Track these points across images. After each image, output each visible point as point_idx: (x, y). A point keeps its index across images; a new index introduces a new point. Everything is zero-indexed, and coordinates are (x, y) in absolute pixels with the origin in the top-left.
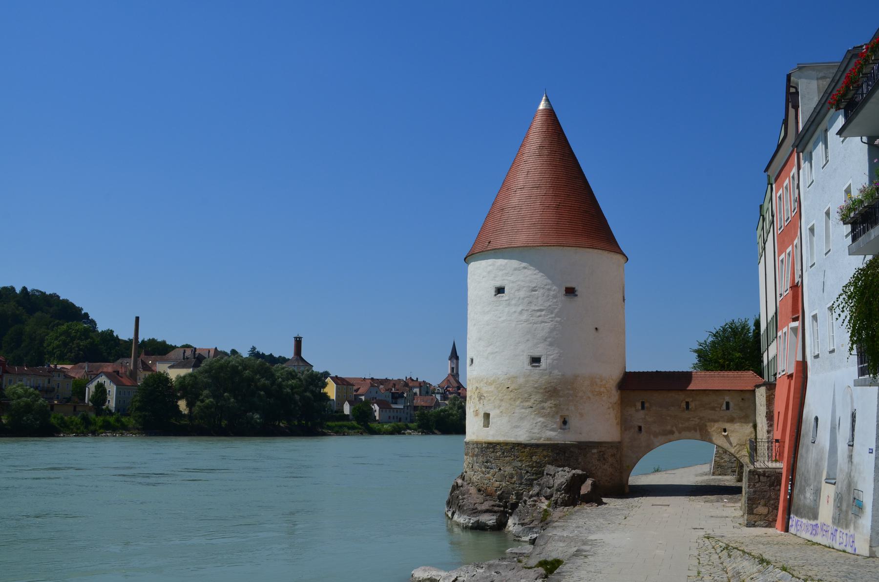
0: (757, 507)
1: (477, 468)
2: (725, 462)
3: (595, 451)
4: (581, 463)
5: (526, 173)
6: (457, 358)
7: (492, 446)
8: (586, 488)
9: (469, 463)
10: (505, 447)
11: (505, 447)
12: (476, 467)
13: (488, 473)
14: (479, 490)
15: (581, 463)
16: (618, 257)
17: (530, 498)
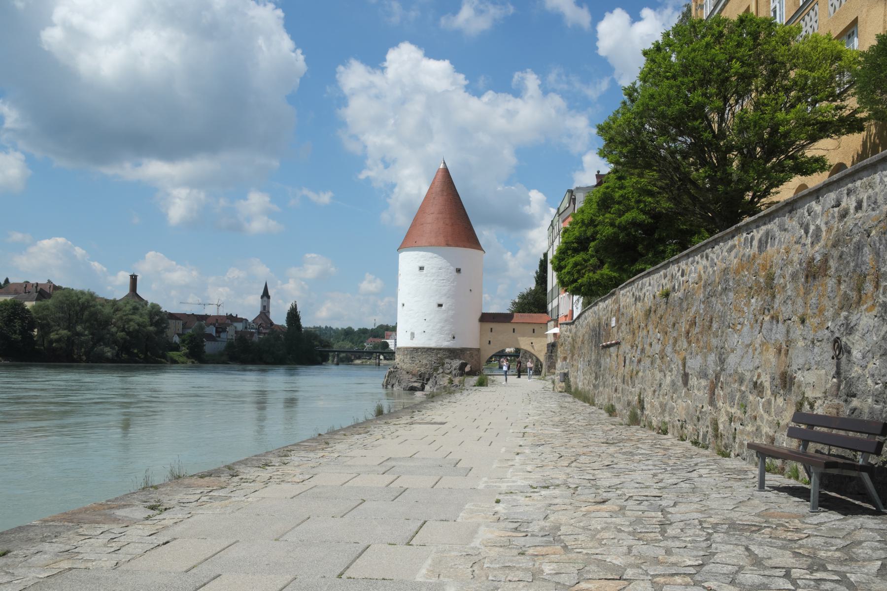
3: (468, 352)
6: (269, 297)
7: (416, 350)
8: (467, 369)
12: (406, 361)
14: (408, 373)
16: (482, 252)
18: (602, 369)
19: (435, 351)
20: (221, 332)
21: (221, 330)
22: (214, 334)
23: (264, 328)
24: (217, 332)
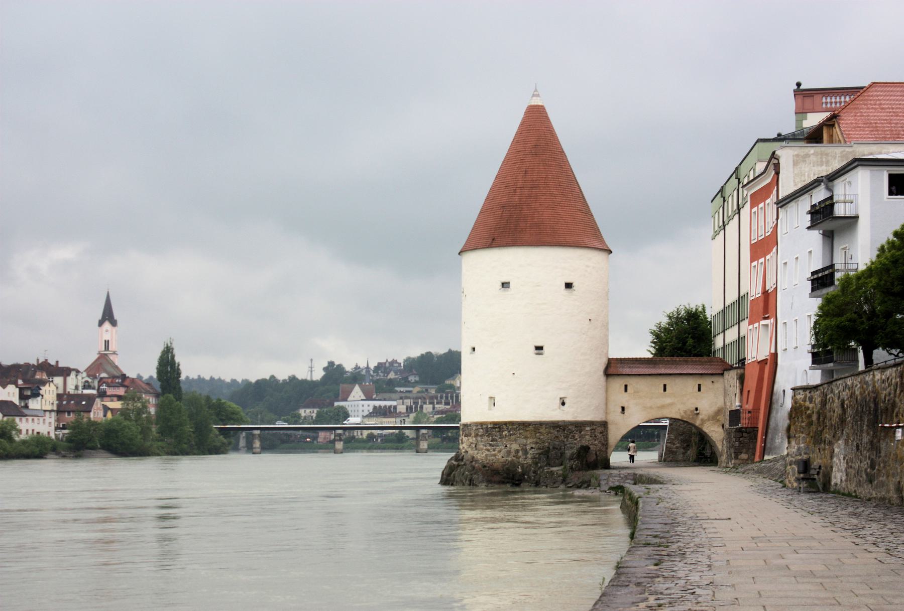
1: (482, 447)
2: (677, 448)
3: (588, 428)
4: (577, 439)
7: (499, 426)
9: (472, 443)
10: (511, 427)
12: (481, 446)
13: (494, 450)
15: (577, 439)
18: (883, 454)
19: (531, 428)
20: (28, 397)
21: (29, 393)
22: (16, 400)
23: (108, 386)
24: (22, 397)
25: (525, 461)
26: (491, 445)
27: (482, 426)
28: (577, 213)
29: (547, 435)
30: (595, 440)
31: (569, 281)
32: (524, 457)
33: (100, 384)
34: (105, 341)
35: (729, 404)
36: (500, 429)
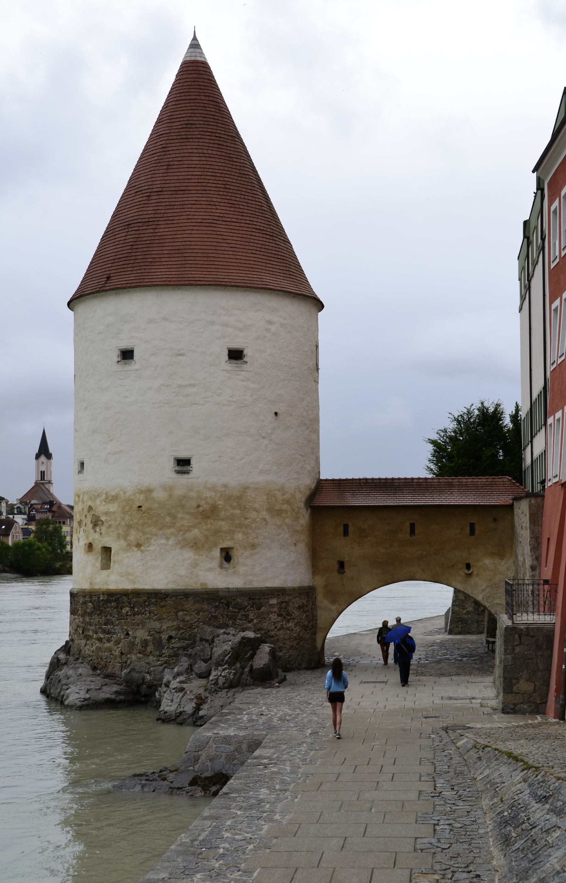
0: (518, 683)
2: (468, 613)
3: (274, 601)
4: (252, 620)
5: (166, 167)
6: (49, 456)
9: (78, 626)
10: (135, 600)
11: (135, 600)
13: (109, 641)
14: (94, 669)
15: (252, 620)
17: (174, 678)
19: (170, 602)
25: (158, 660)
26: (104, 632)
27: (91, 597)
28: (253, 234)
29: (198, 614)
30: (288, 621)
31: (236, 345)
32: (157, 653)
33: (31, 509)
34: (41, 472)
35: (522, 559)
36: (118, 603)
